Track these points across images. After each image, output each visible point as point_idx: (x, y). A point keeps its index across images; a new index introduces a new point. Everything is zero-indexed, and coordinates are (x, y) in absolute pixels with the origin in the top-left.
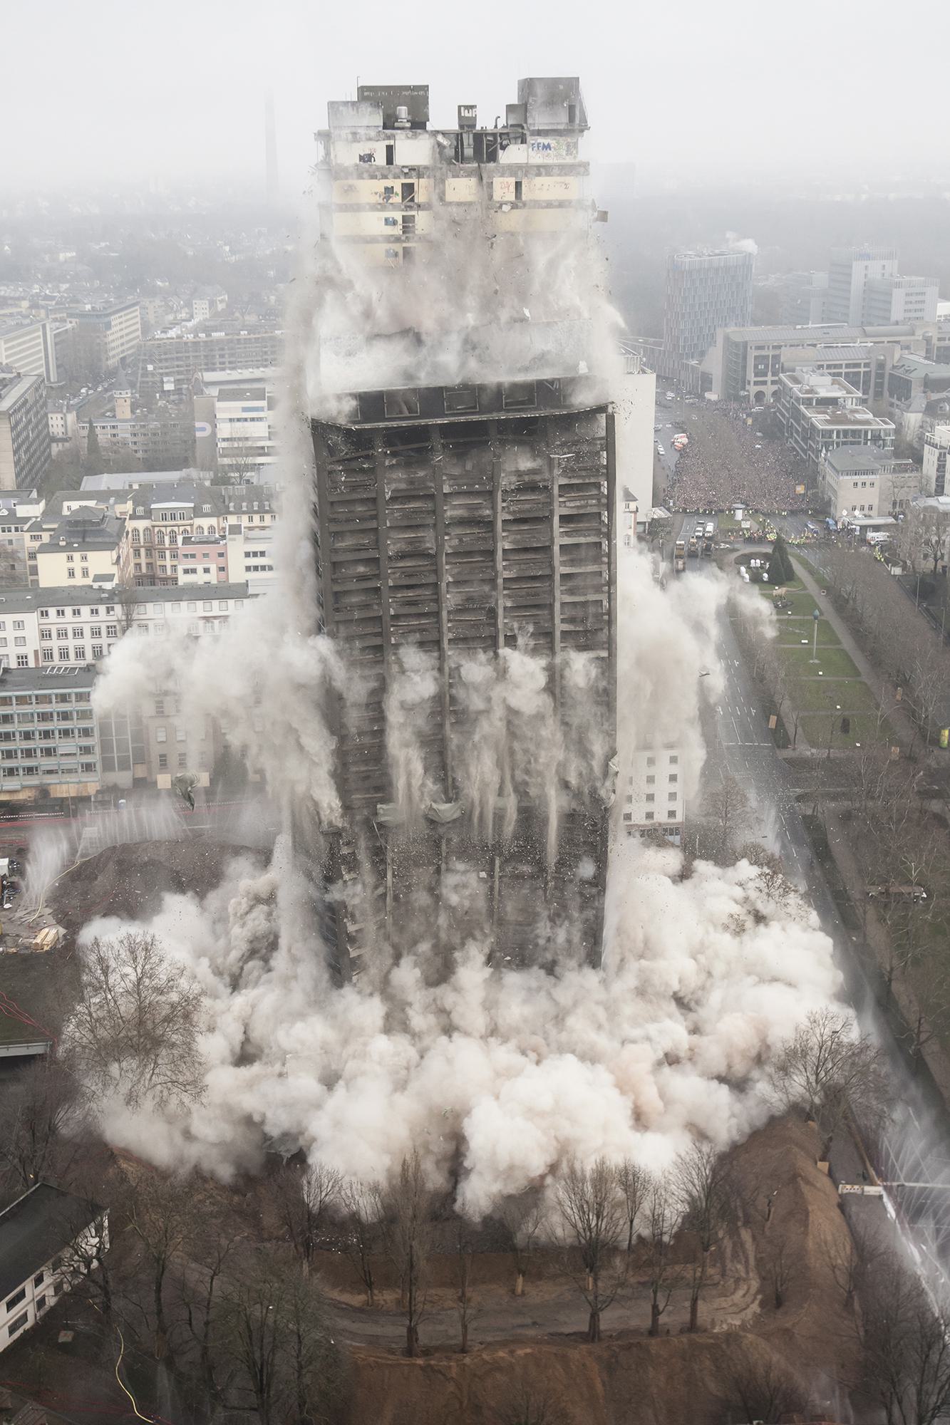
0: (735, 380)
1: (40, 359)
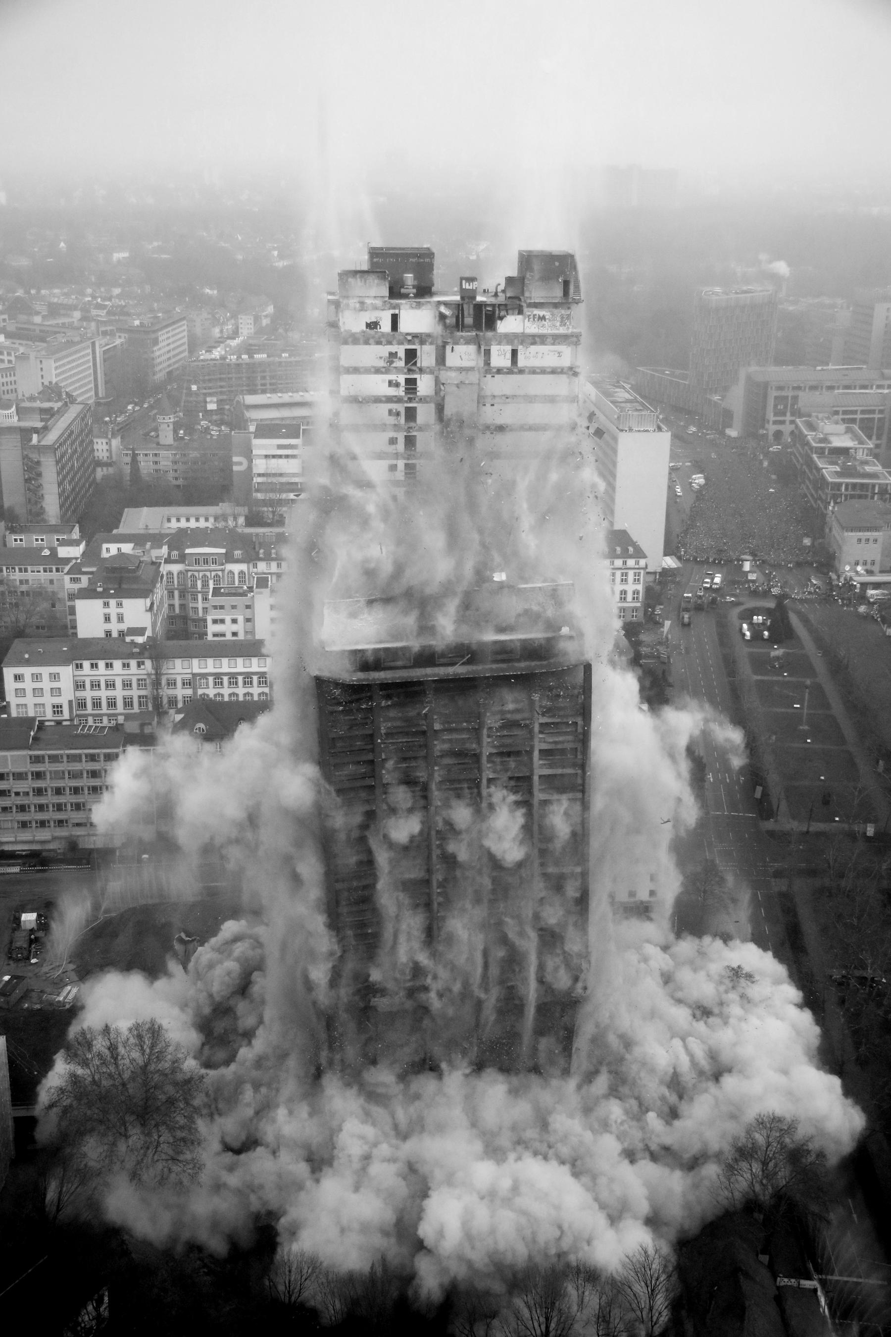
0: (755, 419)
1: (88, 361)
